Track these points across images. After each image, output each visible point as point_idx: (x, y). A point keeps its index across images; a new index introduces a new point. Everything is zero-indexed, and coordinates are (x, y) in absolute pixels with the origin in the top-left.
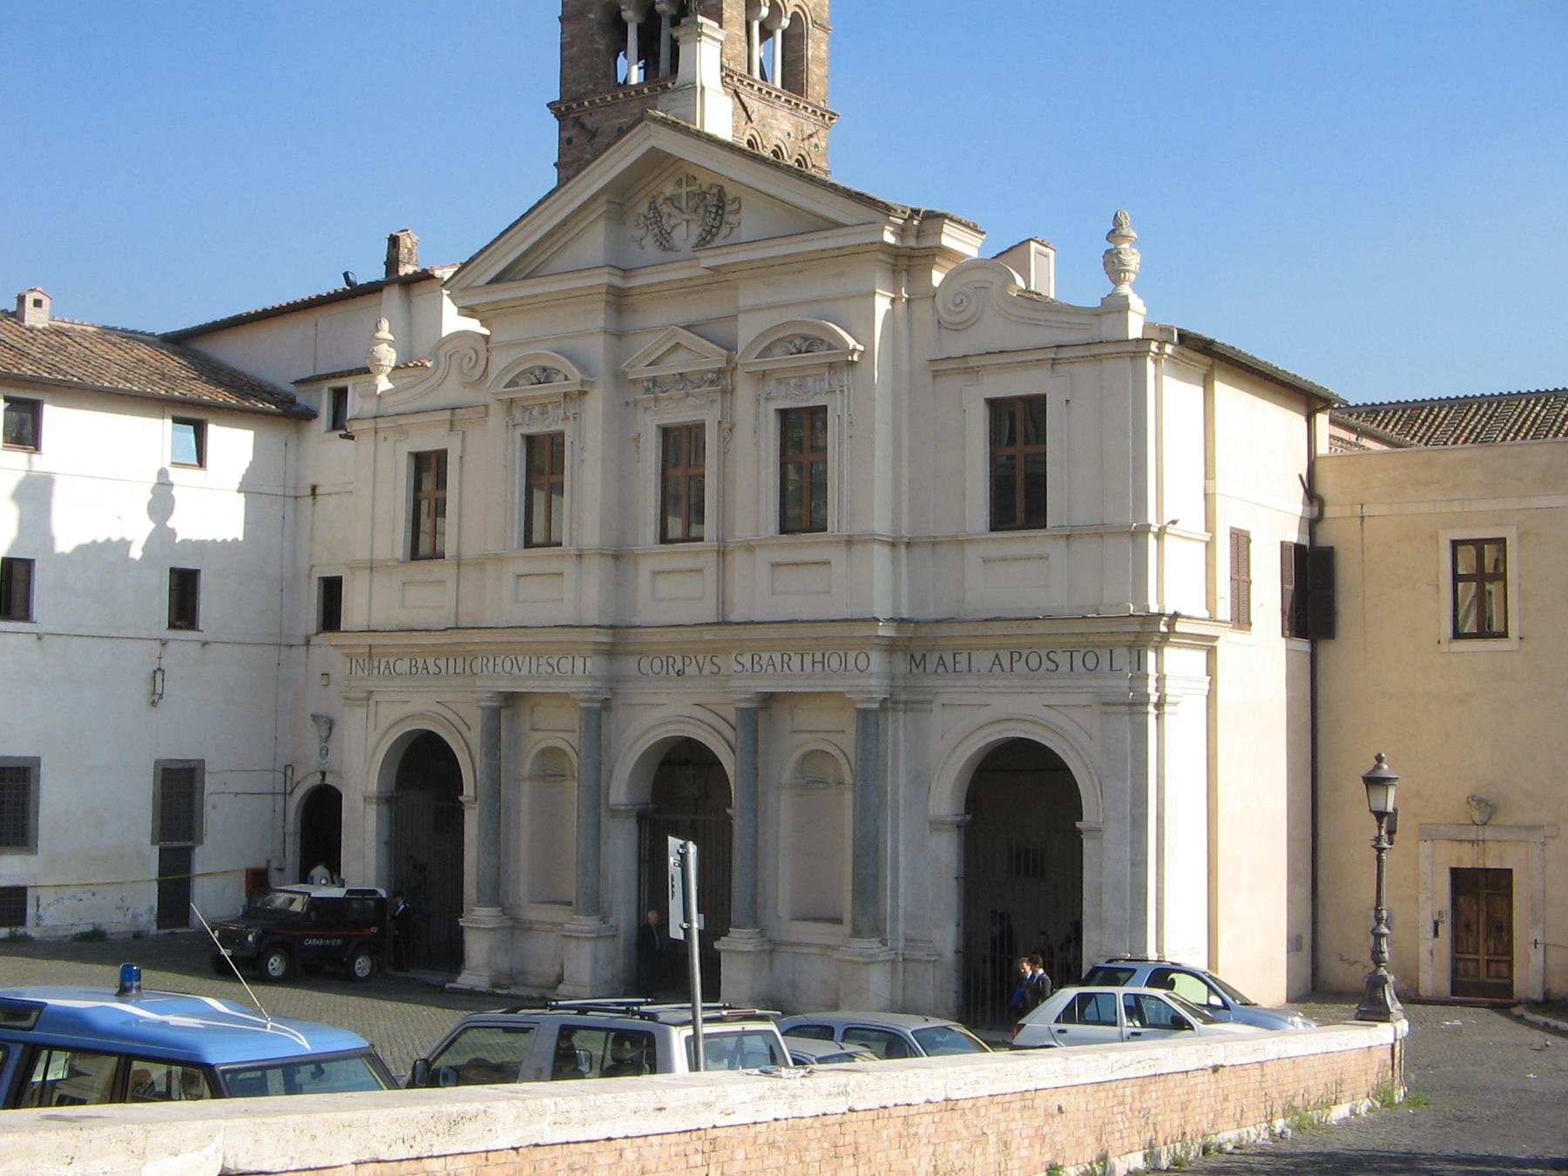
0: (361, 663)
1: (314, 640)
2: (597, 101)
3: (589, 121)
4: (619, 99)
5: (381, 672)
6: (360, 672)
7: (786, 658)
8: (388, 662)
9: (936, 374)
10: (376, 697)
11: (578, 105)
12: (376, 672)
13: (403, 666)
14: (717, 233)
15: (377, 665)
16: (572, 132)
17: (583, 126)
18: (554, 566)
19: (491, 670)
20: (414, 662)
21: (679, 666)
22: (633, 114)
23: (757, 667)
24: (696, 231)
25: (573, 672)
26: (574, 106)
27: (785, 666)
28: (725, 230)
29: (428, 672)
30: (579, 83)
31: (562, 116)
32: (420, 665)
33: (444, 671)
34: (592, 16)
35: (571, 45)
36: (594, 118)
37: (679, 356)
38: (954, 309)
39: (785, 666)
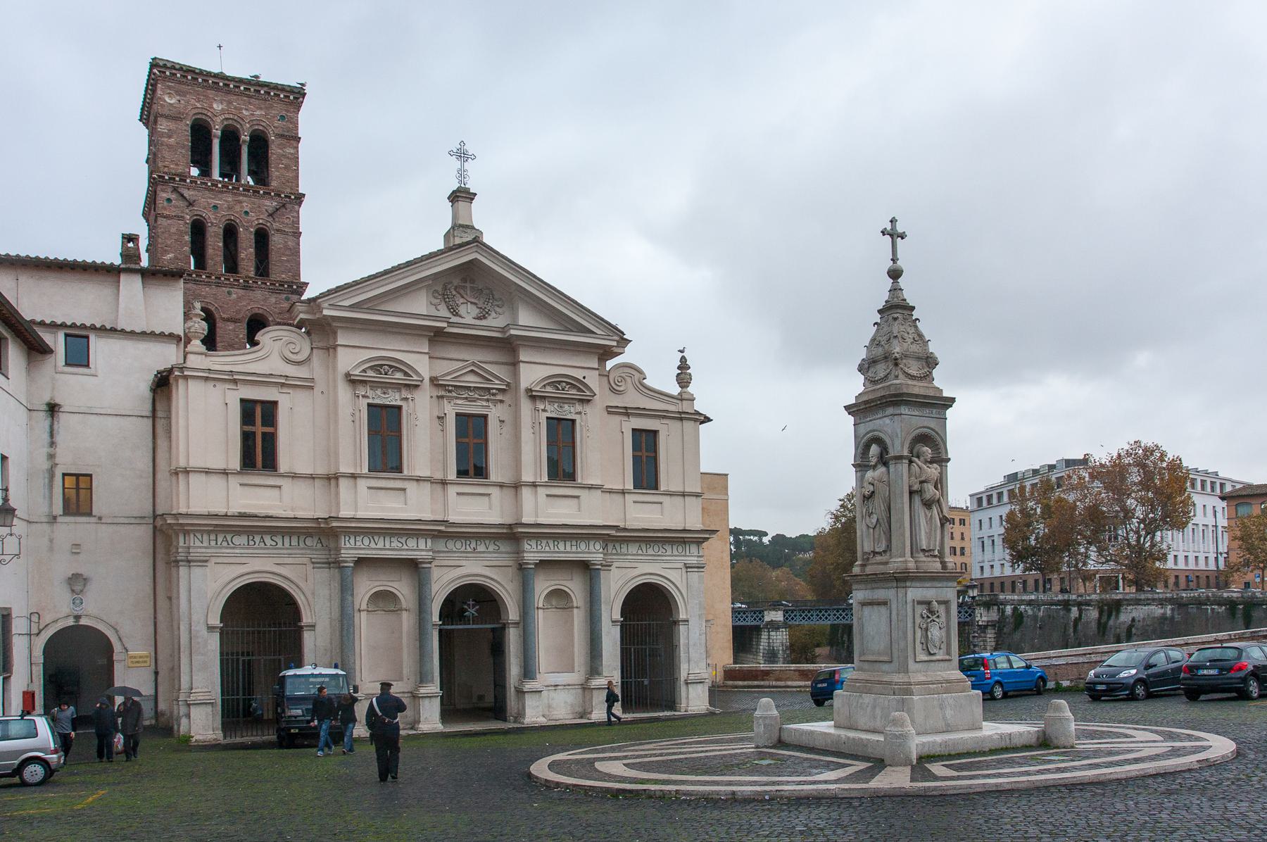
0: (200, 537)
1: (60, 519)
2: (199, 182)
3: (186, 193)
4: (228, 189)
5: (219, 543)
6: (198, 544)
7: (556, 543)
8: (225, 537)
9: (609, 413)
10: (214, 560)
11: (181, 180)
12: (213, 543)
13: (241, 540)
14: (490, 315)
15: (215, 539)
16: (173, 196)
17: (182, 195)
18: (399, 484)
19: (353, 544)
20: (251, 538)
21: (473, 545)
22: (226, 201)
23: (539, 547)
24: (475, 311)
25: (417, 547)
26: (177, 179)
27: (556, 547)
28: (493, 314)
29: (266, 545)
30: (177, 165)
31: (162, 182)
32: (257, 539)
33: (280, 545)
34: (188, 122)
35: (170, 137)
36: (191, 193)
37: (471, 378)
38: (616, 381)
39: (556, 547)
